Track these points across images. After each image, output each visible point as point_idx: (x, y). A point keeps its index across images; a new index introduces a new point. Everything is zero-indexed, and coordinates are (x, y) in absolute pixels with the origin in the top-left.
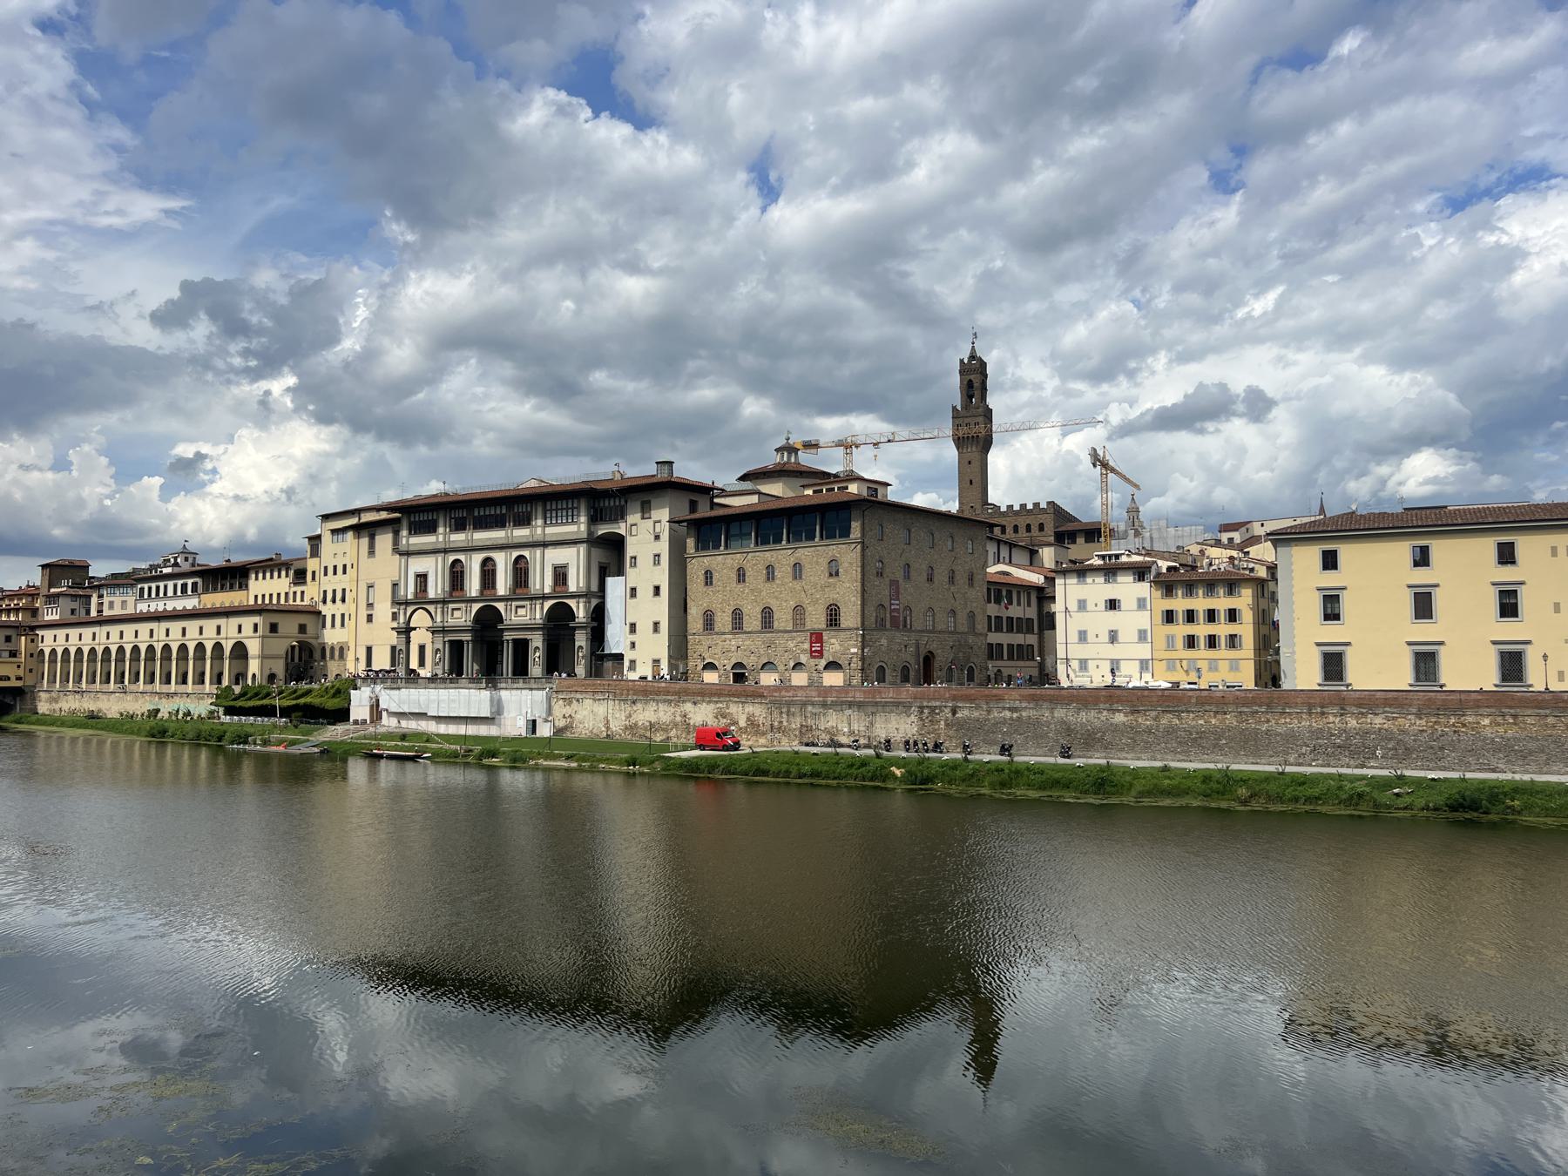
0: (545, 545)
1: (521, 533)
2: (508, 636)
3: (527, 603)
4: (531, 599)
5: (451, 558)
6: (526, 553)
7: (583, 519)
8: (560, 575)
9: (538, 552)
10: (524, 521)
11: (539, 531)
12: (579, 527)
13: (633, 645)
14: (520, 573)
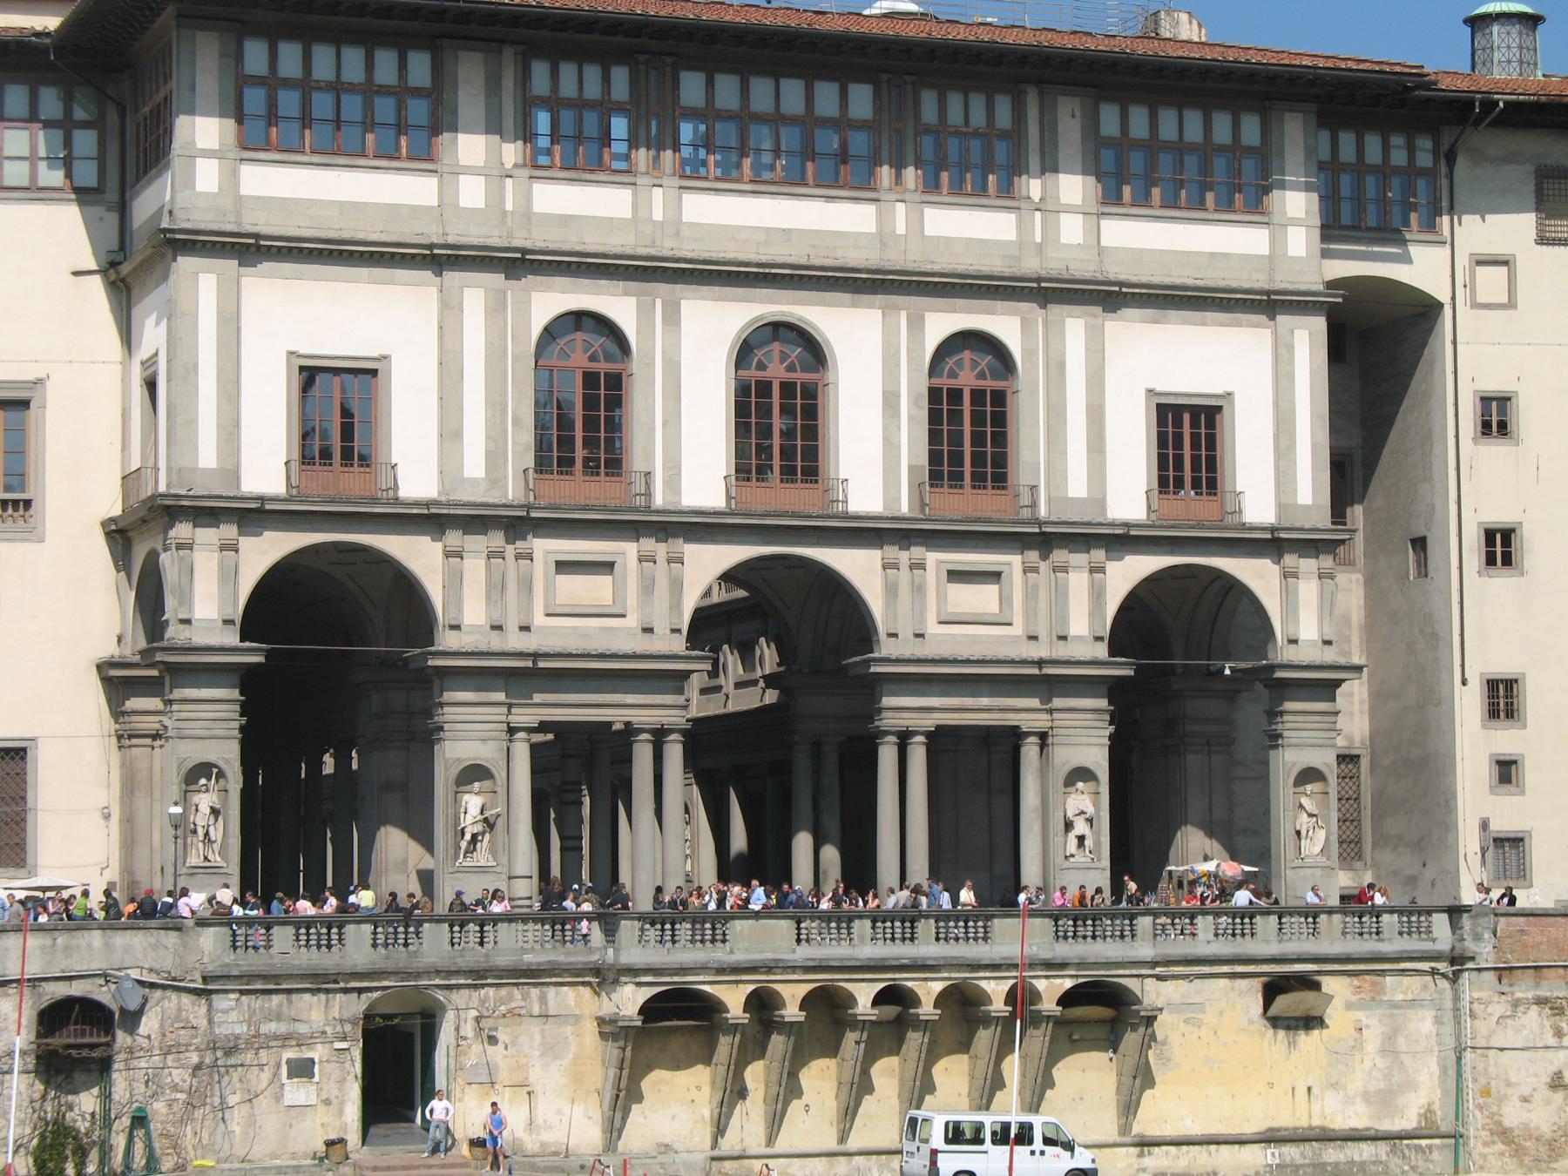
0: (1109, 297)
1: (965, 230)
2: (903, 710)
3: (1012, 562)
4: (1044, 541)
5: (550, 300)
6: (1004, 324)
7: (1297, 204)
8: (1189, 438)
9: (1075, 325)
10: (984, 169)
11: (1072, 229)
12: (1284, 237)
13: (1506, 771)
14: (970, 422)
